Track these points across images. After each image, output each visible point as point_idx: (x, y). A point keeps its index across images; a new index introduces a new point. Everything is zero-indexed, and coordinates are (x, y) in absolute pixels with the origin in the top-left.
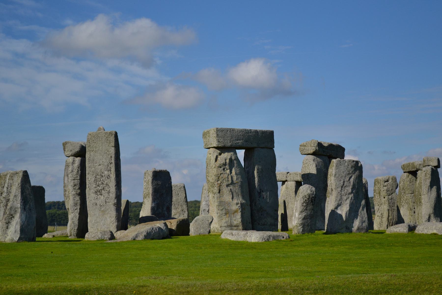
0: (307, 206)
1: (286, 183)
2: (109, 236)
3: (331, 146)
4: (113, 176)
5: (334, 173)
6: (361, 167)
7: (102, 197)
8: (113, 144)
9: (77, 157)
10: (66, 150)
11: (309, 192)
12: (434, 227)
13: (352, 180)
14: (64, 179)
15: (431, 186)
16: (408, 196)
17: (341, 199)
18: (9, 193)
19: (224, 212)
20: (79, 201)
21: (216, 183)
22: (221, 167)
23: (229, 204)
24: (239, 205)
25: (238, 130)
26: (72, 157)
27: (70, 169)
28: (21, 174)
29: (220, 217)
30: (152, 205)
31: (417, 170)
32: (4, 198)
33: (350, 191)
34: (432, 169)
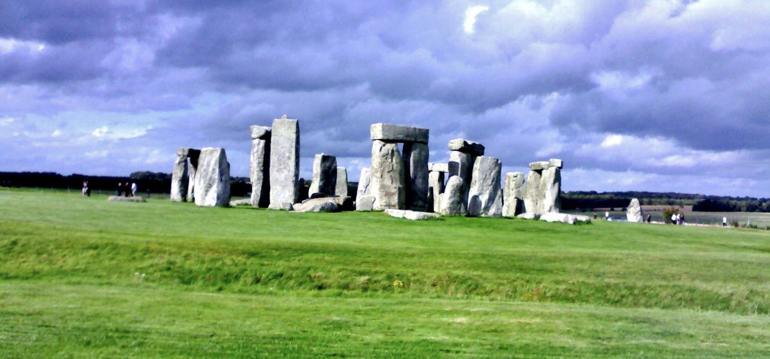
0: (455, 194)
1: (431, 172)
2: (290, 208)
8: (294, 131)
11: (458, 182)
13: (492, 174)
15: (554, 183)
16: (532, 191)
17: (482, 190)
19: (384, 193)
21: (379, 170)
22: (384, 156)
24: (397, 189)
29: (381, 198)
30: (320, 183)
31: (542, 170)
33: (490, 183)
34: (556, 169)
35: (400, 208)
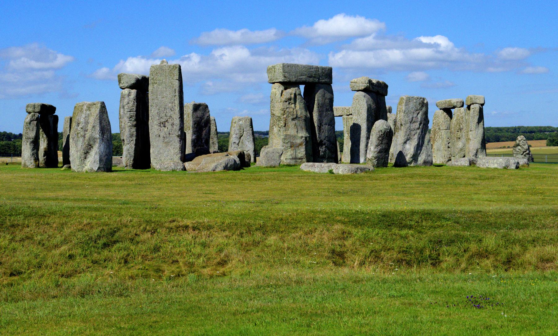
0: (382, 141)
3: (378, 82)
4: (177, 109)
5: (404, 109)
6: (427, 105)
7: (166, 129)
8: (177, 77)
9: (132, 89)
10: (122, 82)
12: (495, 161)
14: (120, 111)
18: (87, 123)
20: (135, 133)
23: (294, 137)
24: (304, 138)
25: (301, 66)
26: (128, 89)
27: (126, 100)
28: (99, 105)
32: (82, 128)
35: (308, 161)
